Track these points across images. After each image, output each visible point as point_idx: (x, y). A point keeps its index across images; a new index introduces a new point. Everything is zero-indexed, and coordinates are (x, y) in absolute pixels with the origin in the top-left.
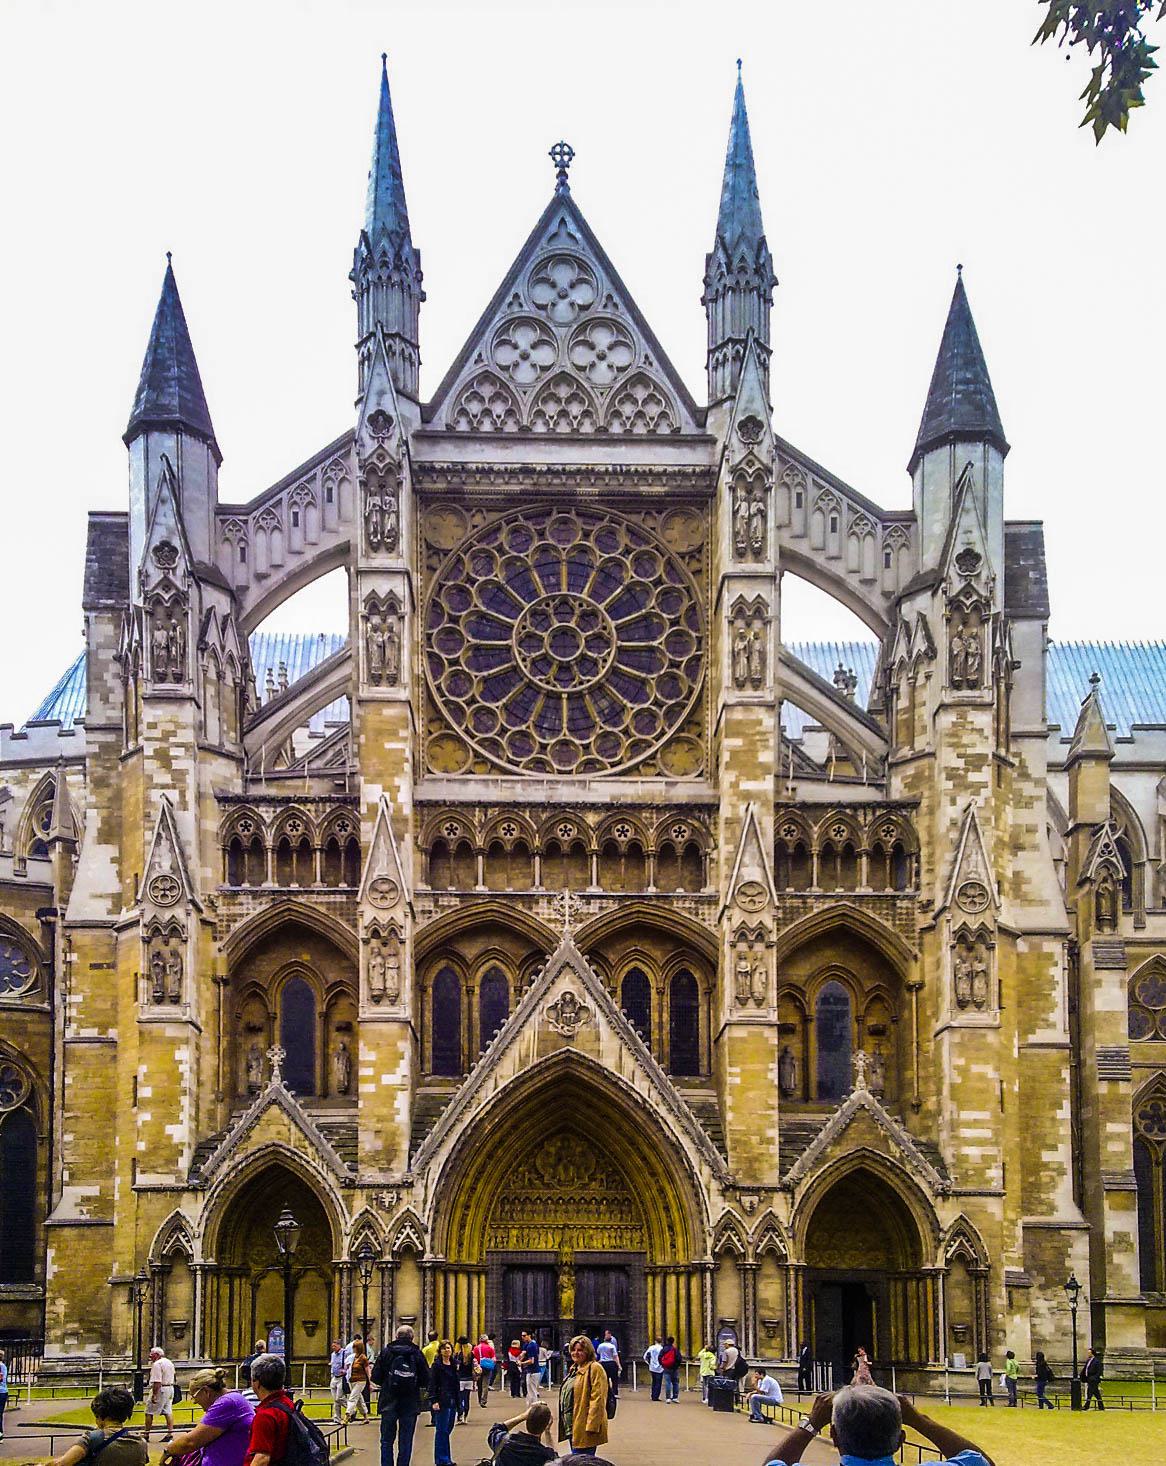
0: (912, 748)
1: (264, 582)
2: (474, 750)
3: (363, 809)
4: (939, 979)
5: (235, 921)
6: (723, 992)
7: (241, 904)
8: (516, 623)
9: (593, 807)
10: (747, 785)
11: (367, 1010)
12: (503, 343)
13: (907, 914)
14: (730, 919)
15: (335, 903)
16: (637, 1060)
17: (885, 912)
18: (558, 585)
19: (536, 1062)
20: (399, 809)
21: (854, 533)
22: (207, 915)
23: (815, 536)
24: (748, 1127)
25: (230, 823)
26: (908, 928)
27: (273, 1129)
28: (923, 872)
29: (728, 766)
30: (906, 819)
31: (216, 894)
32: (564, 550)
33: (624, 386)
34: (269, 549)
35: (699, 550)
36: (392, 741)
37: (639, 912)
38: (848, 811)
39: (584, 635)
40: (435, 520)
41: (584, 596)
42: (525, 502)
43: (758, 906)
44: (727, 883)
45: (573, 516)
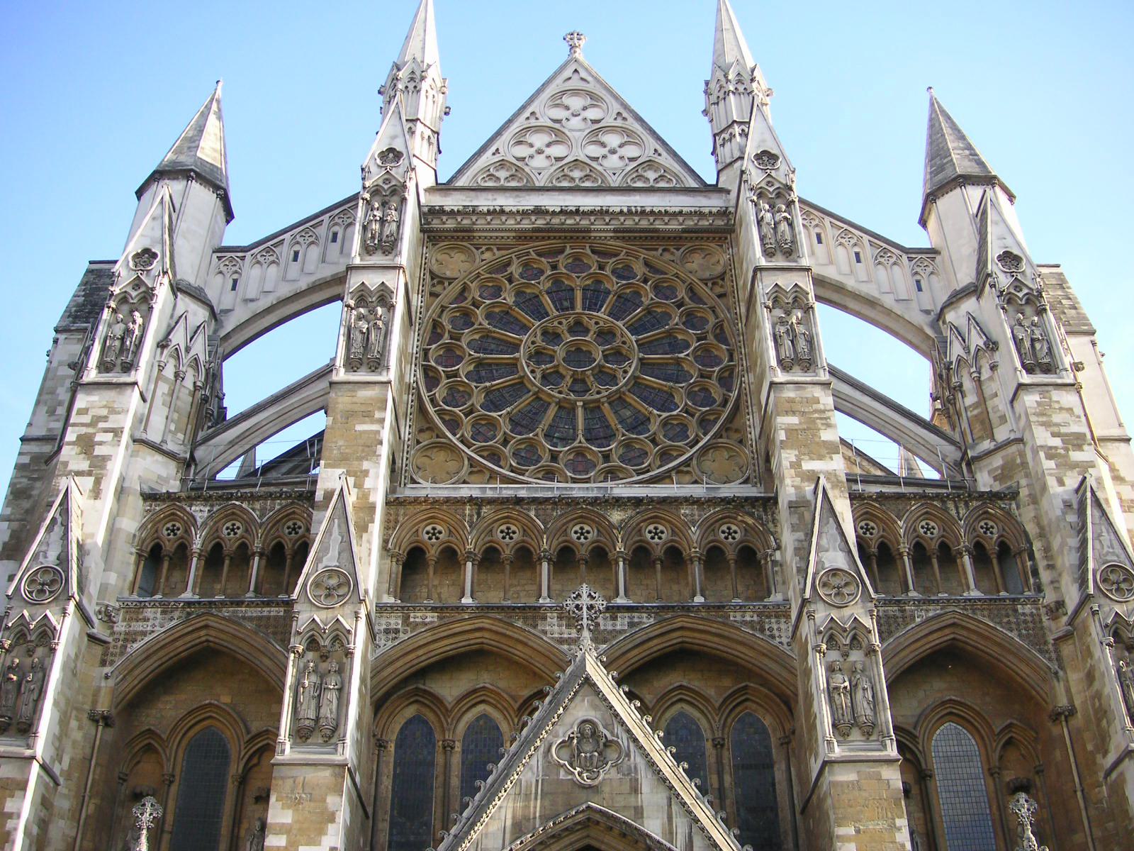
0: (993, 439)
1: (251, 305)
2: (470, 458)
3: (319, 496)
4: (1098, 695)
5: (134, 641)
6: (812, 727)
7: (146, 620)
9: (618, 502)
10: (808, 465)
11: (287, 750)
12: (520, 143)
13: (1033, 622)
14: (811, 616)
15: (269, 618)
17: (1005, 620)
18: (573, 308)
20: (364, 496)
21: (880, 263)
22: (99, 630)
23: (839, 267)
25: (153, 524)
26: (1037, 638)
30: (1008, 513)
31: (117, 605)
32: (578, 282)
33: (636, 169)
34: (263, 279)
35: (722, 277)
36: (364, 423)
37: (681, 628)
39: (601, 348)
40: (440, 257)
41: (599, 314)
45: (588, 251)
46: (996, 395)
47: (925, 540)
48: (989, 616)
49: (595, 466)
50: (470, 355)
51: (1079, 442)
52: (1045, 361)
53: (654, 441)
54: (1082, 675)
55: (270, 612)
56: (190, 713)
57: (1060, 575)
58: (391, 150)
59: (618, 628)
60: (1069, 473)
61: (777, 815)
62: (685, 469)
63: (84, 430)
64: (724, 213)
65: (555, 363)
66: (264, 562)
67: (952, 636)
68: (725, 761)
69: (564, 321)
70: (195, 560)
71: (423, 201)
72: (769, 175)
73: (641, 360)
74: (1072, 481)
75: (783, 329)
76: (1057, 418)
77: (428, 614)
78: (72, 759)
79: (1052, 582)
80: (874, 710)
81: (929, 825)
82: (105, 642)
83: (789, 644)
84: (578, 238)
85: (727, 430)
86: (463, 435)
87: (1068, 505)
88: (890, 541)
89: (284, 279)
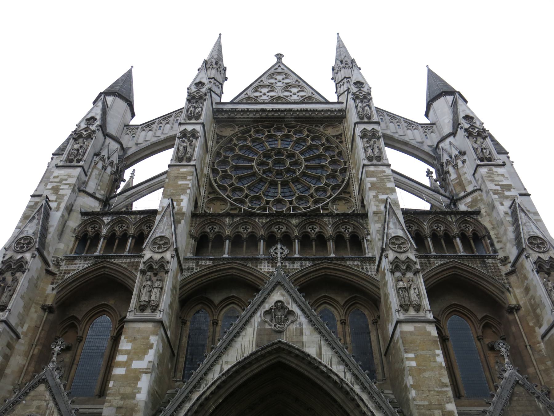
0: (465, 191)
1: (139, 145)
2: (231, 203)
4: (533, 297)
5: (69, 273)
6: (389, 309)
8: (256, 157)
14: (387, 257)
15: (133, 263)
16: (333, 348)
19: (254, 350)
20: (181, 209)
21: (409, 129)
22: (52, 268)
24: (431, 403)
25: (84, 224)
27: (35, 403)
28: (495, 243)
29: (370, 189)
31: (63, 258)
34: (146, 136)
35: (341, 135)
37: (325, 268)
38: (441, 216)
40: (221, 129)
41: (289, 148)
42: (262, 121)
43: (403, 249)
44: (380, 243)
45: (283, 126)
46: (466, 173)
47: (437, 231)
48: (472, 264)
49: (286, 206)
50: (232, 164)
51: (509, 188)
52: (489, 156)
53: (311, 196)
54: (522, 290)
55: (134, 260)
56: (93, 309)
57: (505, 245)
58: (200, 83)
59: (295, 267)
60: (505, 200)
61: (372, 356)
62: (326, 207)
63: (55, 184)
64: (341, 111)
65: (269, 166)
66: (134, 240)
67: (454, 272)
68: (347, 330)
69: (273, 152)
70: (102, 239)
71: (214, 107)
72: (360, 90)
73: (306, 166)
74: (508, 203)
75: (368, 145)
76: (496, 178)
77: (208, 262)
78: (29, 327)
79: (501, 248)
80: (420, 298)
81: (449, 363)
82: (56, 274)
83: (375, 275)
84: (279, 121)
85: (345, 192)
86: (228, 194)
87: (506, 214)
88: (420, 231)
89: (154, 136)
